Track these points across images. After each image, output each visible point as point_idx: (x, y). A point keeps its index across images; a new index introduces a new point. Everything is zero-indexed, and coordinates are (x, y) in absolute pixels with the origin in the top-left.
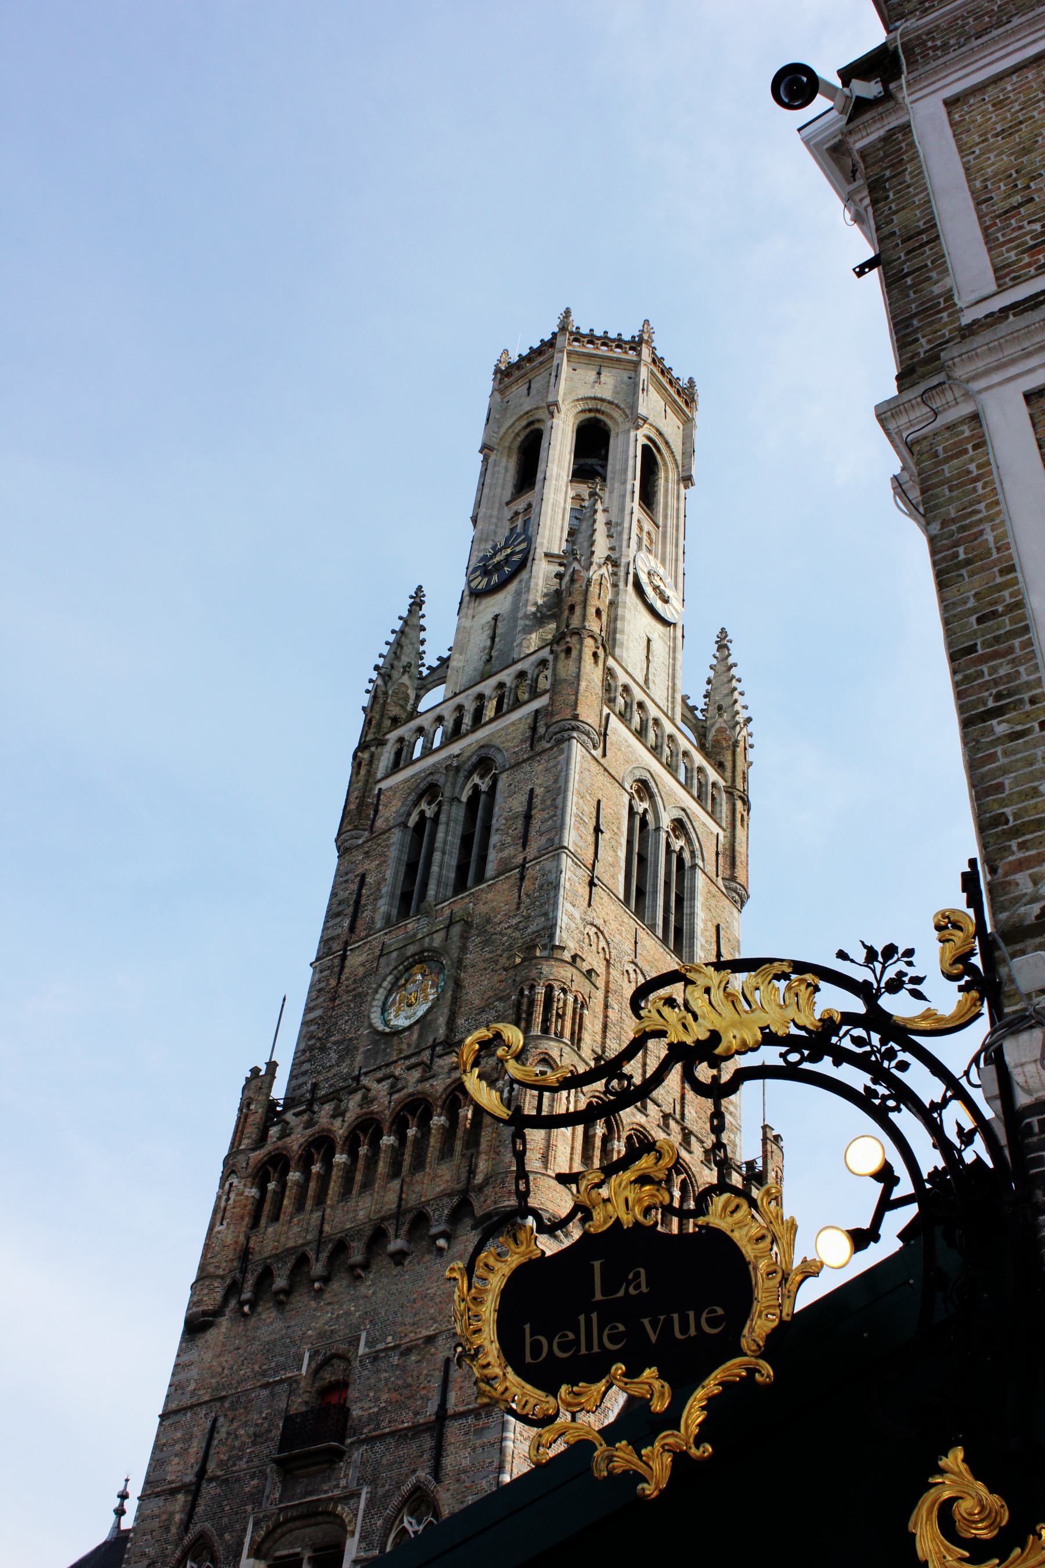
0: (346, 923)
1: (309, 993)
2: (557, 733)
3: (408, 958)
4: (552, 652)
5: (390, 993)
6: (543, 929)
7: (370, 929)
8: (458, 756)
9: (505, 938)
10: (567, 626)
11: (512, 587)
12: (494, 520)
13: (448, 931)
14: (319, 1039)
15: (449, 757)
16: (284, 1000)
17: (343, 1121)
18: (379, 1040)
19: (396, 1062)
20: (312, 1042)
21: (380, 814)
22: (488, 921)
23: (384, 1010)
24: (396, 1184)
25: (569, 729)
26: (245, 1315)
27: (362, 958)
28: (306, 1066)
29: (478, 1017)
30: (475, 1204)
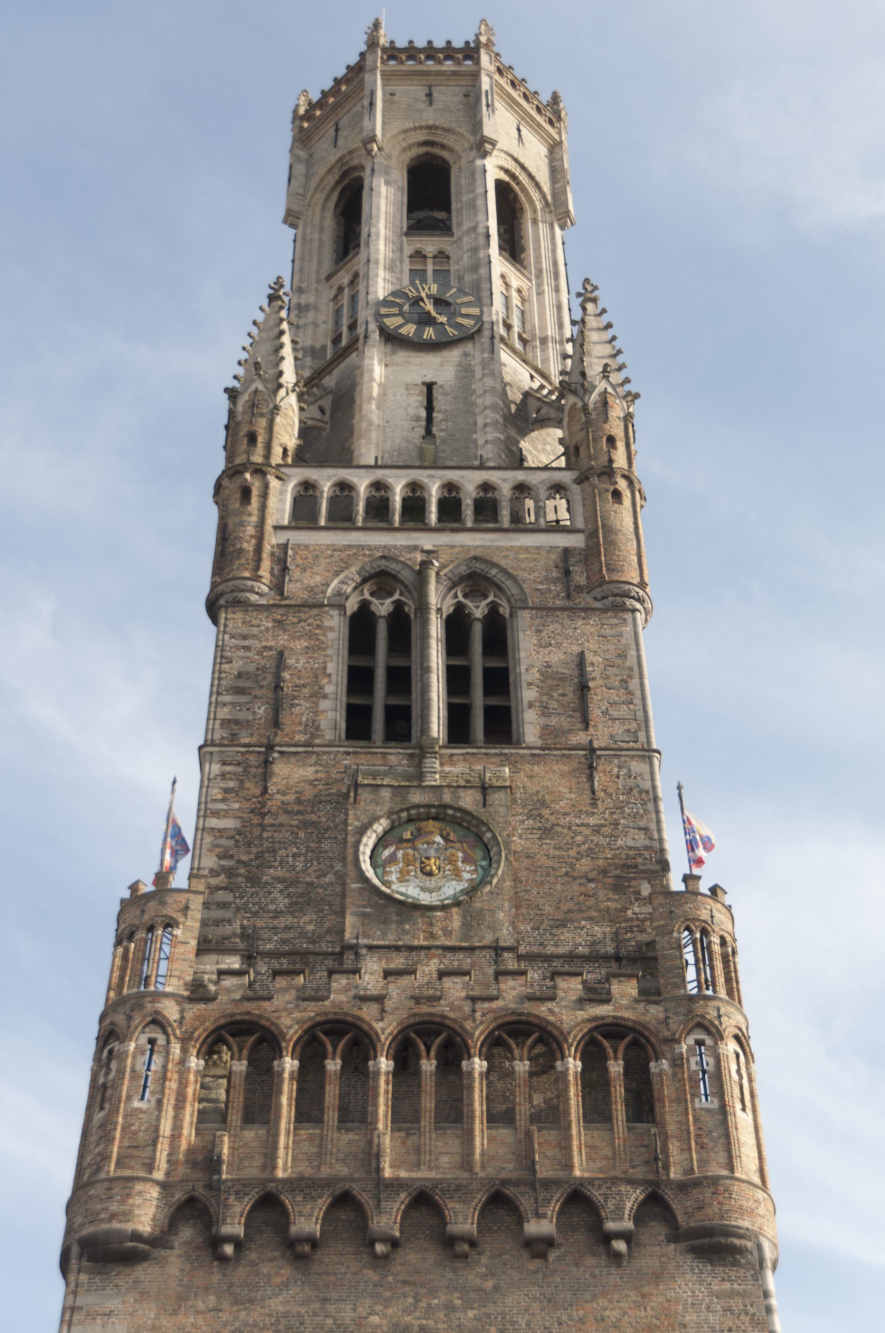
0: (261, 710)
2: (617, 595)
3: (418, 806)
4: (579, 481)
5: (381, 842)
6: (646, 848)
7: (313, 736)
9: (579, 839)
10: (611, 461)
11: (454, 355)
13: (484, 795)
14: (245, 864)
15: (415, 548)
17: (383, 1011)
21: (295, 573)
22: (543, 803)
23: (374, 865)
25: (633, 598)
26: (223, 1259)
27: (309, 772)
28: (222, 896)
29: (554, 931)
30: (674, 1206)
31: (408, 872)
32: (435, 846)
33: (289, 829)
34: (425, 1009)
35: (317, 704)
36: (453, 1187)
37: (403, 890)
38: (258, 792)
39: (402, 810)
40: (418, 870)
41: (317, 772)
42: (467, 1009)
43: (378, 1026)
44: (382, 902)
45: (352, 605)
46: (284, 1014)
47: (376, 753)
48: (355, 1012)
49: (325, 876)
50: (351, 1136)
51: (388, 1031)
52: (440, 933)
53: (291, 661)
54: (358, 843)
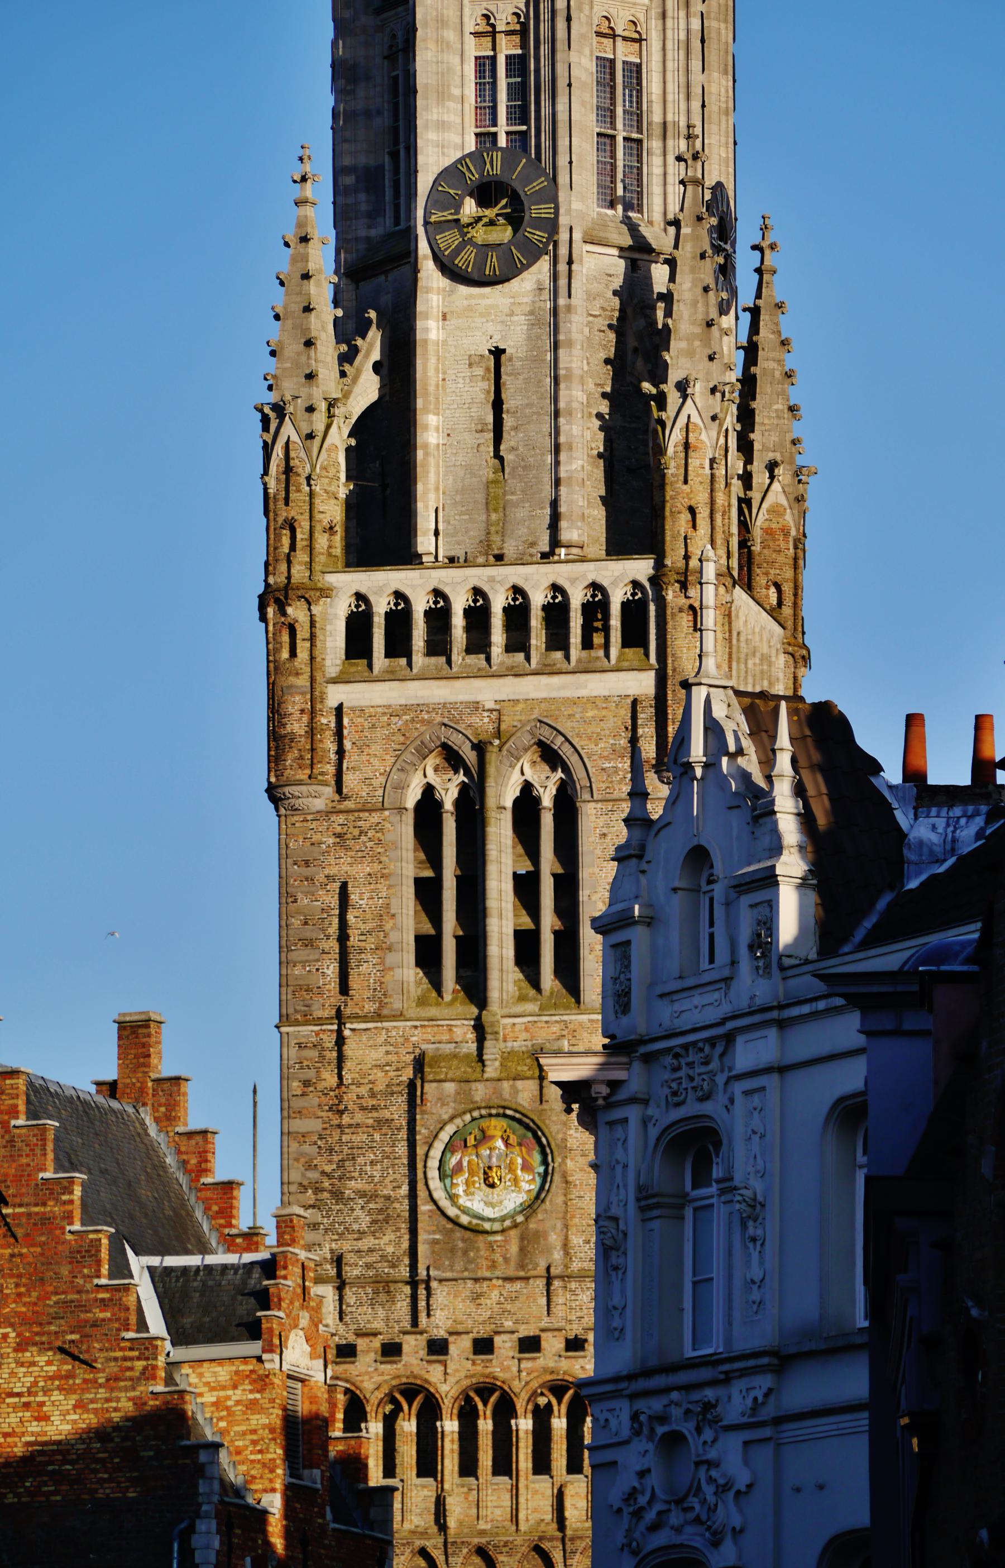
0: (332, 970)
1: (284, 1077)
5: (449, 1148)
8: (491, 711)
10: (687, 557)
12: (451, 35)
14: (328, 1175)
15: (476, 706)
16: (255, 1092)
17: (446, 1373)
18: (452, 1231)
19: (490, 1280)
20: (313, 1175)
24: (543, 1485)
27: (378, 1055)
31: (474, 1183)
32: (497, 1151)
33: (365, 1129)
34: (479, 1368)
35: (382, 963)
36: (502, 1543)
37: (468, 1204)
38: (334, 1081)
39: (464, 1113)
40: (482, 1181)
41: (388, 1053)
42: (515, 1369)
43: (444, 1388)
44: (450, 1226)
45: (413, 796)
46: (366, 1378)
47: (442, 1026)
48: (423, 1373)
49: (400, 1187)
50: (426, 1492)
51: (450, 1394)
52: (501, 1259)
53: (354, 898)
54: (427, 1155)
